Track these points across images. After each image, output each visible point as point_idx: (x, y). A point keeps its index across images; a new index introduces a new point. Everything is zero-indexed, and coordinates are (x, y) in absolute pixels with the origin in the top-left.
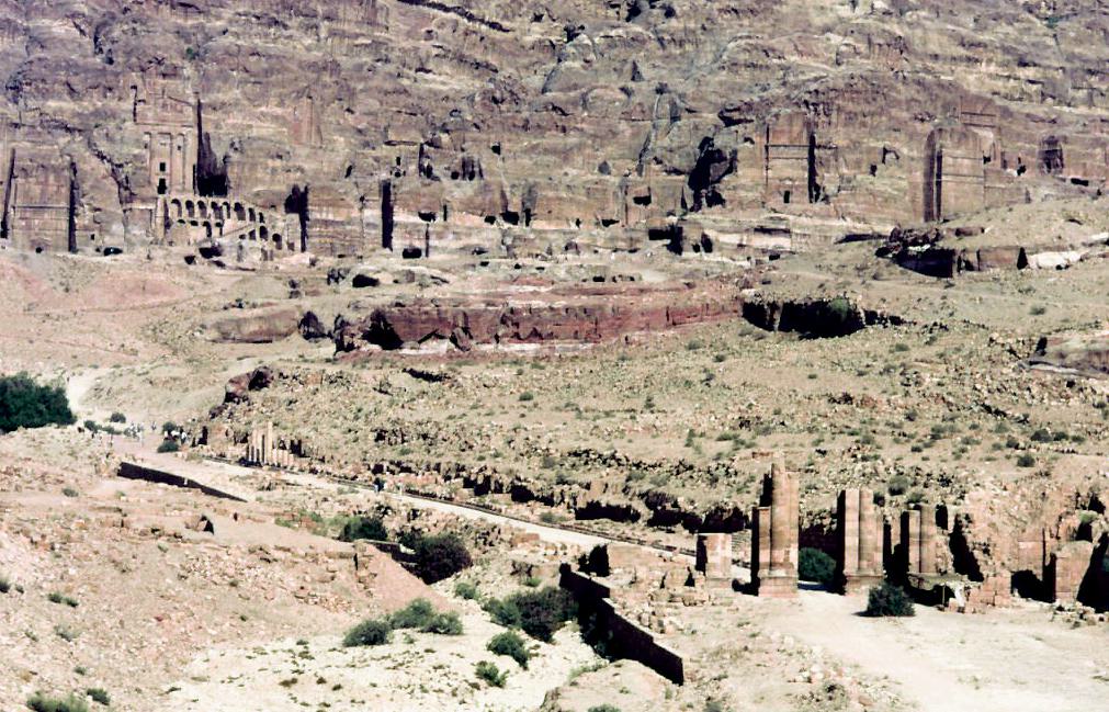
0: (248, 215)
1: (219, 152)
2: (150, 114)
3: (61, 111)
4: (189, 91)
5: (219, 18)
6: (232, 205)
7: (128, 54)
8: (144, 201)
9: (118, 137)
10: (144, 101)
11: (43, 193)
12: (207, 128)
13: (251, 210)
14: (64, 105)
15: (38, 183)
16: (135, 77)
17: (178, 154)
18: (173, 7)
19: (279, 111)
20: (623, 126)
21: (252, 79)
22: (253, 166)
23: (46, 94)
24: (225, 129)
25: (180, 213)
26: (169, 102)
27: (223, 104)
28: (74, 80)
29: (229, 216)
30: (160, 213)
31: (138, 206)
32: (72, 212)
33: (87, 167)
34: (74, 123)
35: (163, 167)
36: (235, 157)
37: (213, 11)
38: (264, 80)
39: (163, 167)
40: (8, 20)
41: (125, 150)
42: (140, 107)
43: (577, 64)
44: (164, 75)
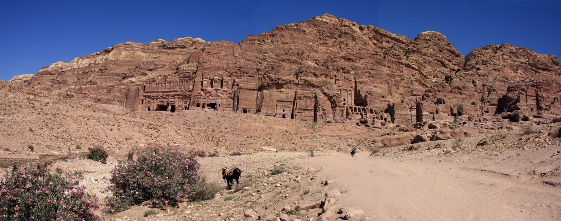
1: (363, 95)
2: (341, 84)
3: (312, 80)
4: (353, 78)
5: (359, 63)
7: (333, 66)
8: (340, 107)
9: (331, 88)
11: (306, 104)
12: (358, 88)
16: (335, 73)
17: (349, 97)
18: (345, 59)
19: (381, 86)
20: (476, 93)
22: (374, 99)
23: (307, 75)
24: (364, 90)
25: (352, 111)
28: (316, 72)
30: (345, 111)
31: (337, 108)
32: (315, 111)
33: (321, 97)
34: (316, 84)
35: (344, 100)
36: (369, 96)
39: (344, 100)
40: (296, 61)
41: (333, 92)
42: (337, 81)
43: (458, 80)
44: (345, 73)
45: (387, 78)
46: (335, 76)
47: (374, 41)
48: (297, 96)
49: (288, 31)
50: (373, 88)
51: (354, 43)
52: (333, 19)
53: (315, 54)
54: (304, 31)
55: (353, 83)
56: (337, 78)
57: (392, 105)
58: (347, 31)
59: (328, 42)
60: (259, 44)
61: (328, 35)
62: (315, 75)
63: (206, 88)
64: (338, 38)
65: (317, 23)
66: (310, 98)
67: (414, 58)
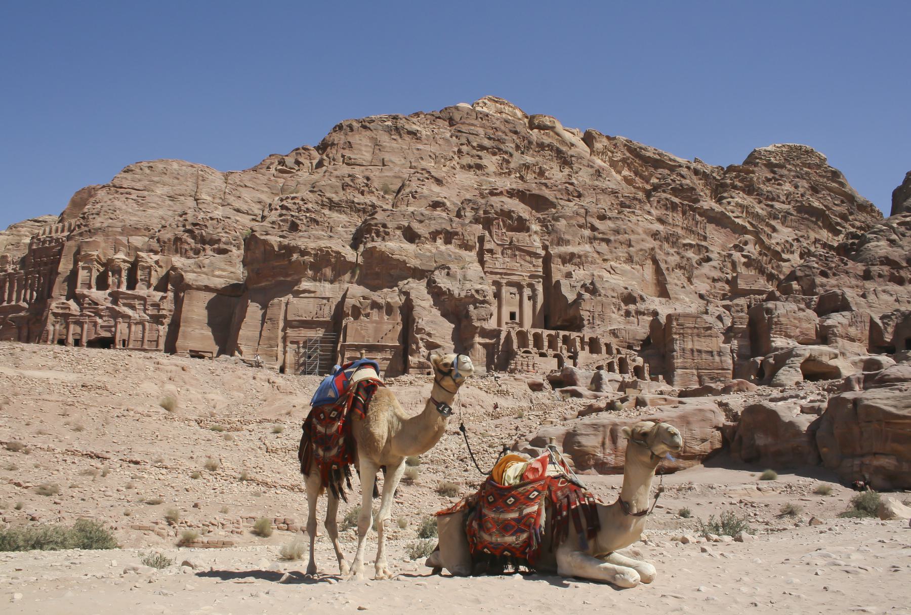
0: (604, 349)
6: (586, 339)
10: (491, 251)
11: (377, 330)
12: (556, 276)
13: (608, 346)
14: (402, 245)
15: (372, 322)
21: (600, 236)
26: (517, 253)
27: (572, 255)
29: (583, 349)
34: (413, 263)
35: (512, 316)
37: (562, 202)
38: (612, 238)
45: (650, 243)
46: (481, 239)
47: (626, 172)
48: (349, 302)
49: (368, 133)
50: (606, 275)
51: (567, 170)
52: (507, 109)
53: (436, 188)
54: (413, 134)
55: (540, 262)
56: (487, 246)
57: (663, 320)
58: (547, 140)
59: (484, 162)
60: (281, 171)
61: (487, 143)
62: (411, 236)
63: (86, 292)
64: (517, 154)
65: (457, 116)
66: (389, 309)
67: (740, 201)
